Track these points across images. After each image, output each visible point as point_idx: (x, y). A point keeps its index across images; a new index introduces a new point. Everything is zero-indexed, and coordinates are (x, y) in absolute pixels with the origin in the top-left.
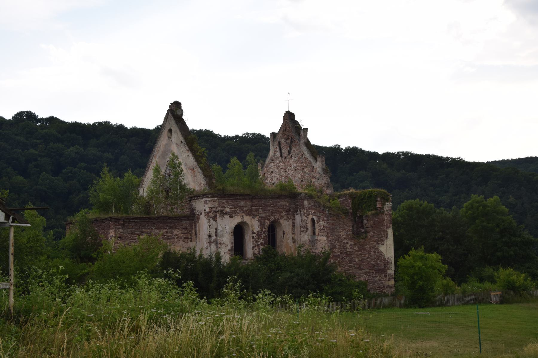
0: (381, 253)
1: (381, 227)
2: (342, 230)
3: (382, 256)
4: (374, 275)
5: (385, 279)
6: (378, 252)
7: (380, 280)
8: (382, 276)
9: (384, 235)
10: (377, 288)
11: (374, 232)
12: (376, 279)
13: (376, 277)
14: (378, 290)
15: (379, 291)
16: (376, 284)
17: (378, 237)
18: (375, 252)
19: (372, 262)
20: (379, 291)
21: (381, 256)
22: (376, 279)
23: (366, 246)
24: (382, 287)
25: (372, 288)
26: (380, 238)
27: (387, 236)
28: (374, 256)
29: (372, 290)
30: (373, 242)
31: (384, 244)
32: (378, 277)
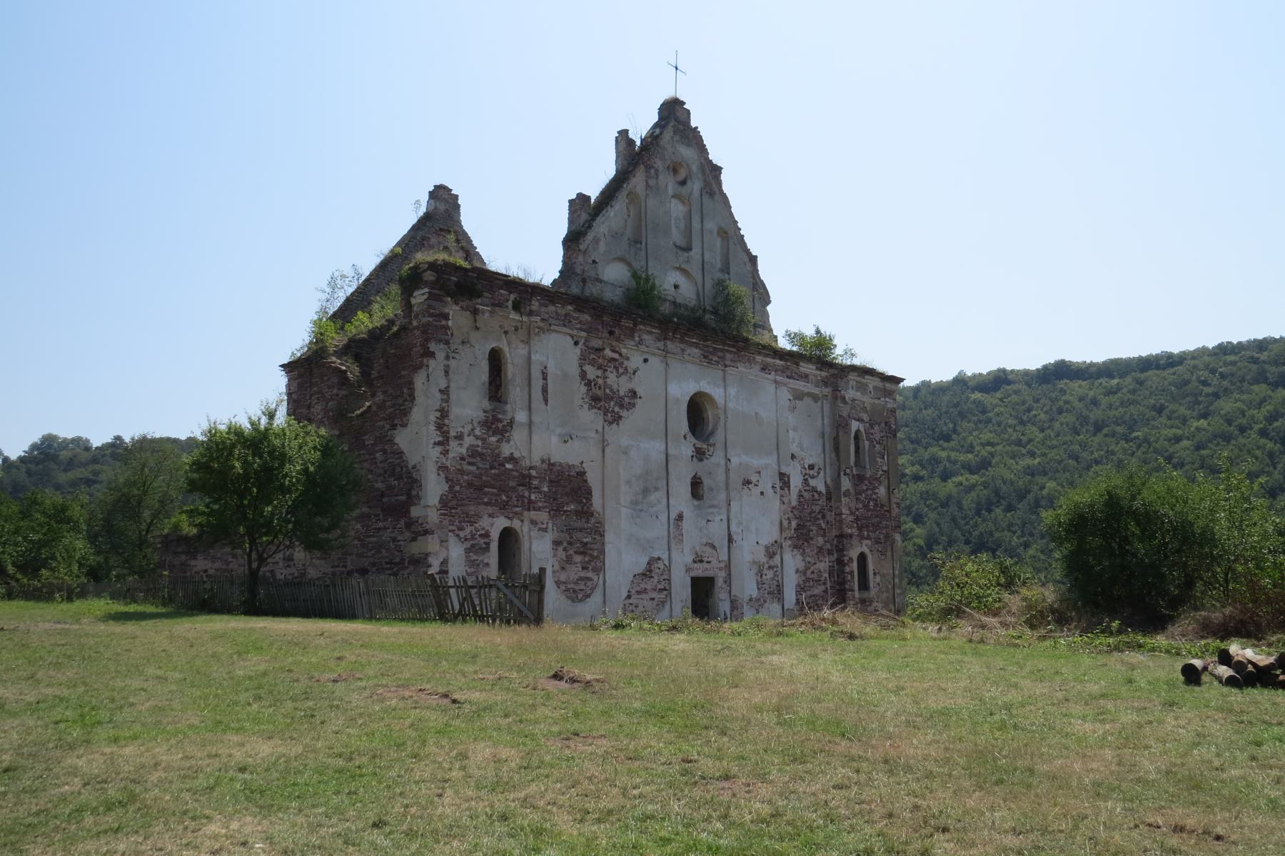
0: (400, 453)
1: (403, 373)
2: (318, 399)
3: (403, 461)
4: (380, 524)
5: (408, 535)
6: (391, 453)
7: (394, 540)
8: (398, 526)
9: (409, 396)
10: (387, 563)
11: (384, 392)
12: (386, 536)
13: (385, 528)
14: (387, 569)
15: (390, 572)
16: (383, 551)
17: (394, 405)
18: (385, 452)
19: (379, 485)
20: (390, 572)
21: (399, 464)
22: (386, 536)
23: (366, 437)
24: (397, 560)
25: (374, 564)
26: (400, 405)
27: (414, 399)
28: (382, 465)
29: (374, 569)
30: (381, 423)
31: (407, 424)
32: (390, 530)
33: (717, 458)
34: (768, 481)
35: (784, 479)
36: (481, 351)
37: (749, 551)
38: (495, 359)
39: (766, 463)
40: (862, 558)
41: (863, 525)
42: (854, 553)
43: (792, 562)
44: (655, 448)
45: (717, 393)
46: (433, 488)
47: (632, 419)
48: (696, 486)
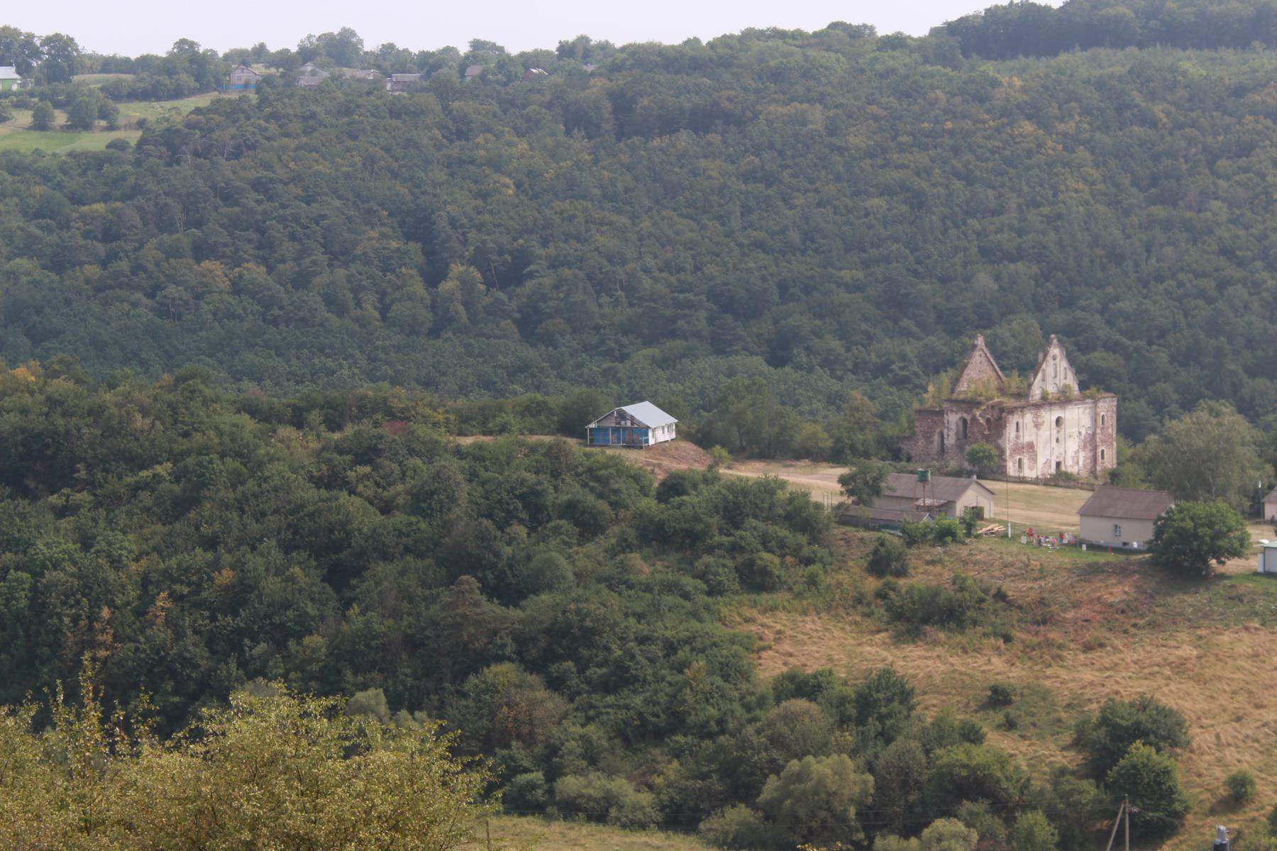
33: (1062, 432)
34: (1077, 434)
35: (1080, 433)
36: (1015, 422)
37: (1070, 453)
38: (1017, 423)
39: (1075, 430)
40: (1103, 451)
41: (1103, 442)
42: (1099, 450)
43: (1082, 454)
44: (1048, 433)
45: (1062, 415)
46: (1008, 452)
47: (1043, 428)
48: (1057, 440)
